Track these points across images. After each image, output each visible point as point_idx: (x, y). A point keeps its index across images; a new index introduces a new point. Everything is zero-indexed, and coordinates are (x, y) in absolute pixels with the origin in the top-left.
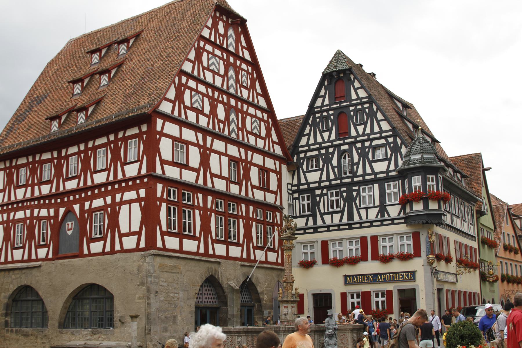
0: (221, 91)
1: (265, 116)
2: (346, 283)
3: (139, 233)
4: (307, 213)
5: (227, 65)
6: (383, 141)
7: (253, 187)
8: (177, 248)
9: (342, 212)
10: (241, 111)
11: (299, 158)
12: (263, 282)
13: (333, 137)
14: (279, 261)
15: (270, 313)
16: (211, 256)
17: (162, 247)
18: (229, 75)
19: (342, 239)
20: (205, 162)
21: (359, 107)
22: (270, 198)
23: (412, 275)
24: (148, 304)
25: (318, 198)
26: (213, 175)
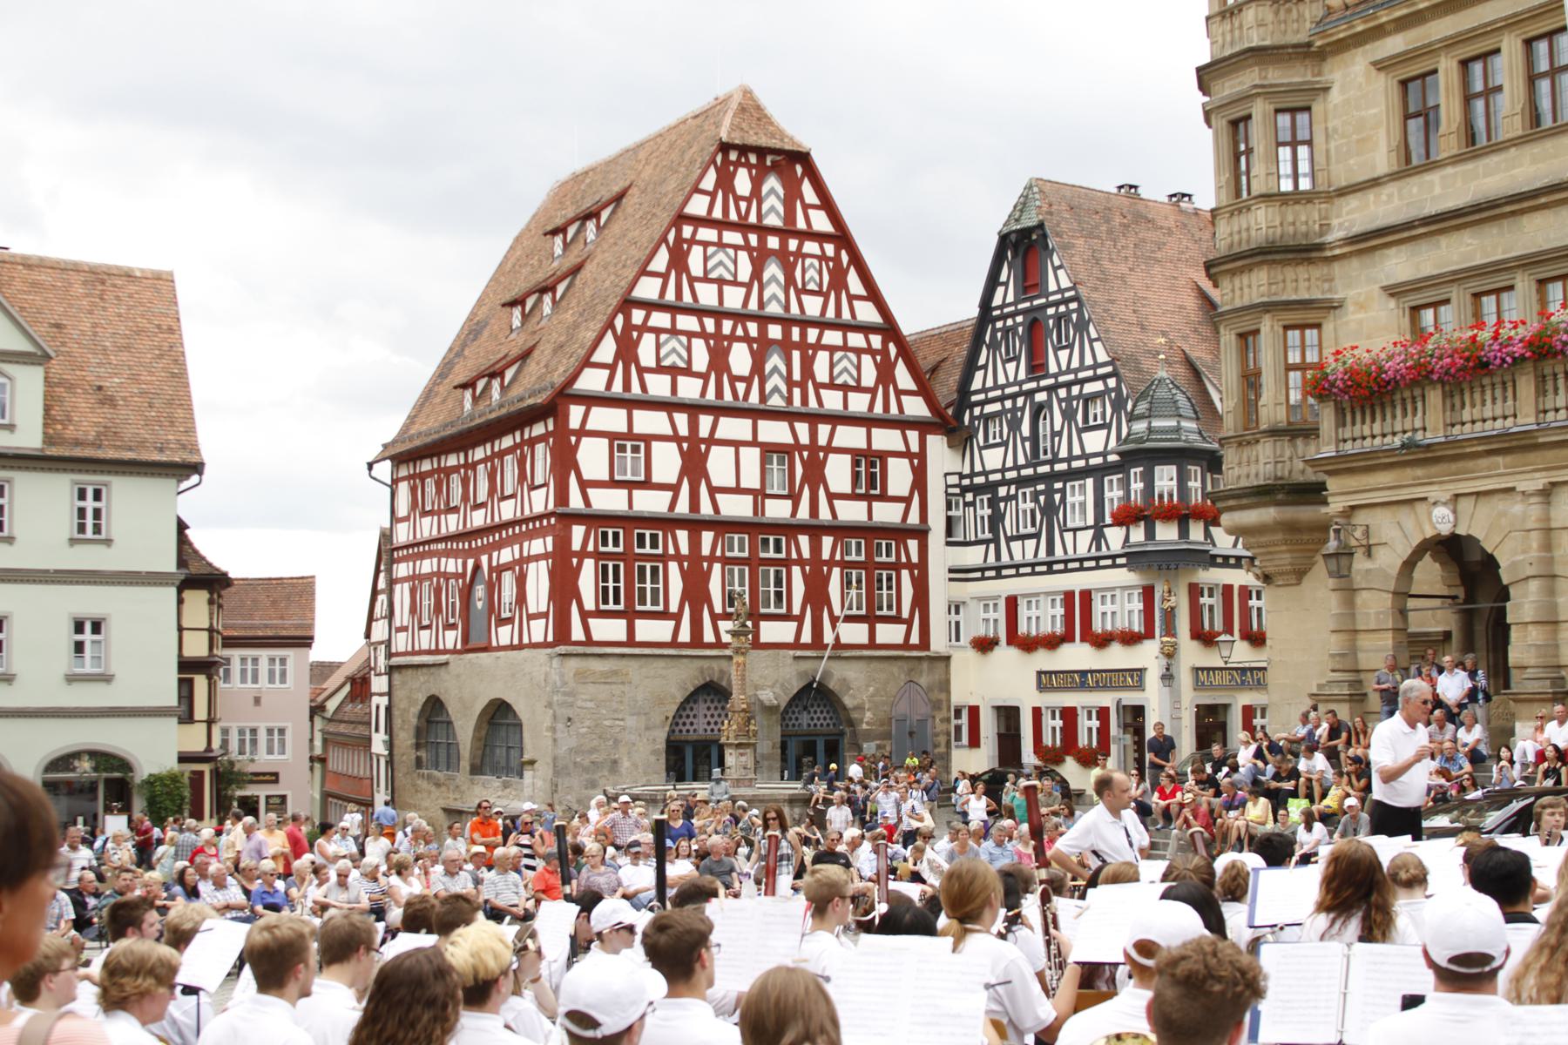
0: (740, 317)
1: (876, 341)
2: (1041, 687)
3: (545, 615)
4: (988, 535)
5: (759, 259)
6: (1098, 386)
7: (831, 497)
8: (622, 636)
9: (1037, 536)
10: (803, 345)
11: (972, 418)
12: (859, 687)
13: (1022, 375)
14: (915, 639)
15: (879, 747)
16: (710, 646)
17: (583, 638)
18: (766, 276)
19: (1037, 595)
20: (694, 466)
21: (1062, 309)
22: (888, 514)
23: (1136, 677)
24: (555, 740)
25: (1002, 505)
26: (713, 491)
